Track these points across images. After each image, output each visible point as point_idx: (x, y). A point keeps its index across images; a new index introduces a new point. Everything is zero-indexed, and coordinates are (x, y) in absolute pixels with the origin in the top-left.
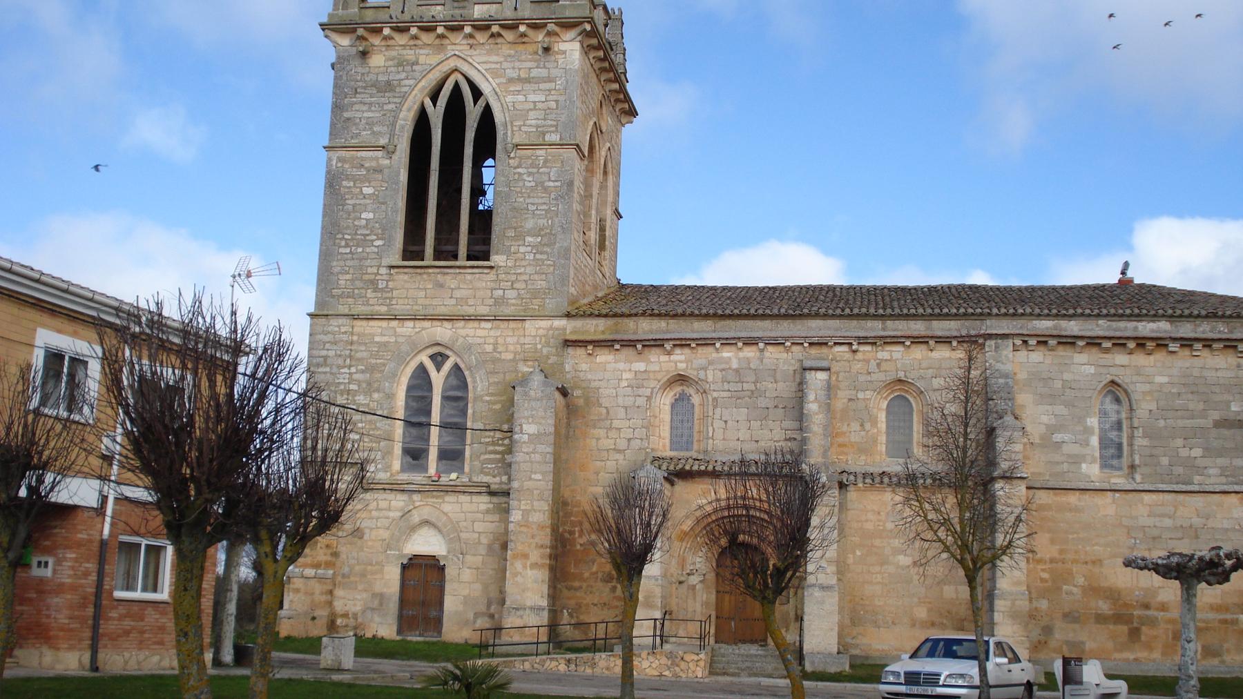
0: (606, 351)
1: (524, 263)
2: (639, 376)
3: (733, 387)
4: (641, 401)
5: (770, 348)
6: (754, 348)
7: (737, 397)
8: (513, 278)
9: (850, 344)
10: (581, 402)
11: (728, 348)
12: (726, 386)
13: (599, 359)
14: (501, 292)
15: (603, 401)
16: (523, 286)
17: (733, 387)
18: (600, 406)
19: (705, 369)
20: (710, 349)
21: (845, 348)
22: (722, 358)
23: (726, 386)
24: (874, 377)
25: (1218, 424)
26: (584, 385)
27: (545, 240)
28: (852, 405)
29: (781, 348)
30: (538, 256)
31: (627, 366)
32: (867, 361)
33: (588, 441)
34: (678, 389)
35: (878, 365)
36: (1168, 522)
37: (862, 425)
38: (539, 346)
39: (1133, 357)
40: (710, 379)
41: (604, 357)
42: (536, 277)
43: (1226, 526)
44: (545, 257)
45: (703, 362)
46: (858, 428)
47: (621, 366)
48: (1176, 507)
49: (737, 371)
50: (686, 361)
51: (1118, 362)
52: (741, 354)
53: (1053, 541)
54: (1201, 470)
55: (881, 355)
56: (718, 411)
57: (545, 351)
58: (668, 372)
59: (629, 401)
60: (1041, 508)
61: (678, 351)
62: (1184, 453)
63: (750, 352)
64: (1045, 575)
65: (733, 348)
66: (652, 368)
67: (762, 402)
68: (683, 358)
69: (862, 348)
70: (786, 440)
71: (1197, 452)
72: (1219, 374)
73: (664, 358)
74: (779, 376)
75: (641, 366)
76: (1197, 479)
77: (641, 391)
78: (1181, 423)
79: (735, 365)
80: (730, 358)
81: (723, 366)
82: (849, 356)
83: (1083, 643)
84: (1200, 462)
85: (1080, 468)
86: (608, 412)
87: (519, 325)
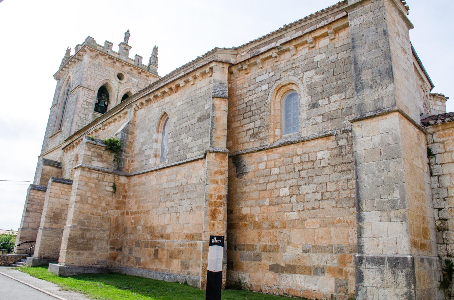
25: (199, 120)
36: (173, 184)
39: (171, 96)
43: (195, 182)
48: (177, 175)
51: (166, 102)
53: (136, 202)
54: (189, 150)
60: (135, 185)
62: (185, 141)
64: (133, 221)
71: (190, 139)
72: (202, 90)
76: (188, 155)
78: (185, 125)
83: (140, 259)
84: (190, 146)
85: (149, 161)
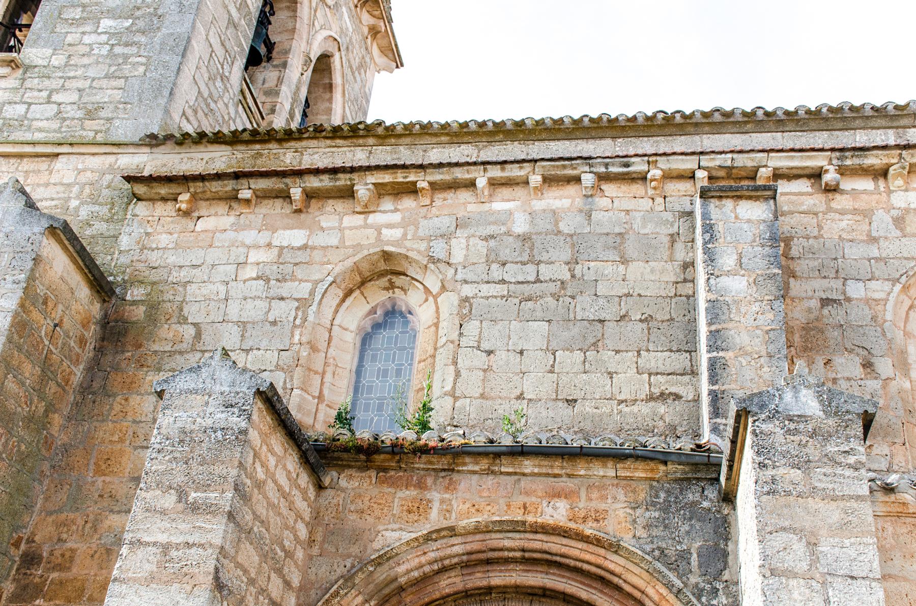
0: (222, 208)
1: (86, 61)
2: (287, 256)
3: (512, 273)
4: (282, 310)
5: (610, 189)
6: (572, 189)
7: (524, 298)
8: (55, 84)
9: (816, 175)
10: (140, 312)
11: (506, 192)
12: (497, 272)
13: (201, 225)
14: (21, 109)
15: (194, 313)
16: (74, 97)
17: (512, 273)
18: (183, 320)
19: (447, 237)
20: (464, 195)
21: (803, 185)
22: (492, 213)
23: (497, 272)
24: (889, 248)
26: (154, 276)
27: (141, 24)
28: (833, 315)
29: (637, 188)
30: (118, 50)
31: (263, 238)
32: (867, 214)
33: (135, 400)
34: (377, 296)
35: (899, 222)
37: (867, 365)
38: (74, 203)
40: (458, 256)
41: (216, 220)
42: (104, 83)
44: (134, 50)
45: (445, 222)
46: (859, 371)
47: (249, 236)
49: (525, 238)
50: (403, 225)
52: (538, 205)
55: (900, 200)
56: (472, 328)
57: (84, 213)
58: (358, 247)
59: (254, 311)
61: (387, 204)
63: (562, 200)
65: (519, 192)
66: (320, 239)
67: (586, 307)
68: (396, 217)
69: (847, 184)
70: (651, 398)
73: (352, 220)
74: (631, 249)
75: (295, 237)
77: (286, 289)
79: (520, 226)
80: (510, 213)
81: (491, 230)
82: (817, 201)
86: (198, 335)
87: (43, 165)
